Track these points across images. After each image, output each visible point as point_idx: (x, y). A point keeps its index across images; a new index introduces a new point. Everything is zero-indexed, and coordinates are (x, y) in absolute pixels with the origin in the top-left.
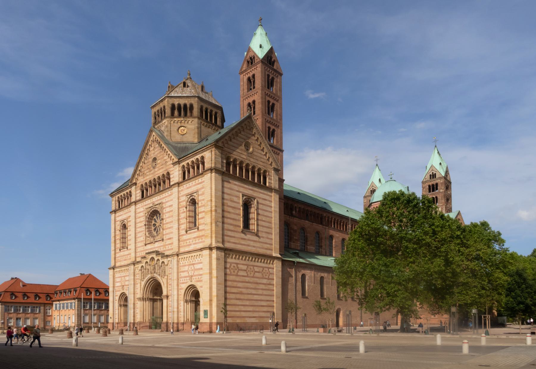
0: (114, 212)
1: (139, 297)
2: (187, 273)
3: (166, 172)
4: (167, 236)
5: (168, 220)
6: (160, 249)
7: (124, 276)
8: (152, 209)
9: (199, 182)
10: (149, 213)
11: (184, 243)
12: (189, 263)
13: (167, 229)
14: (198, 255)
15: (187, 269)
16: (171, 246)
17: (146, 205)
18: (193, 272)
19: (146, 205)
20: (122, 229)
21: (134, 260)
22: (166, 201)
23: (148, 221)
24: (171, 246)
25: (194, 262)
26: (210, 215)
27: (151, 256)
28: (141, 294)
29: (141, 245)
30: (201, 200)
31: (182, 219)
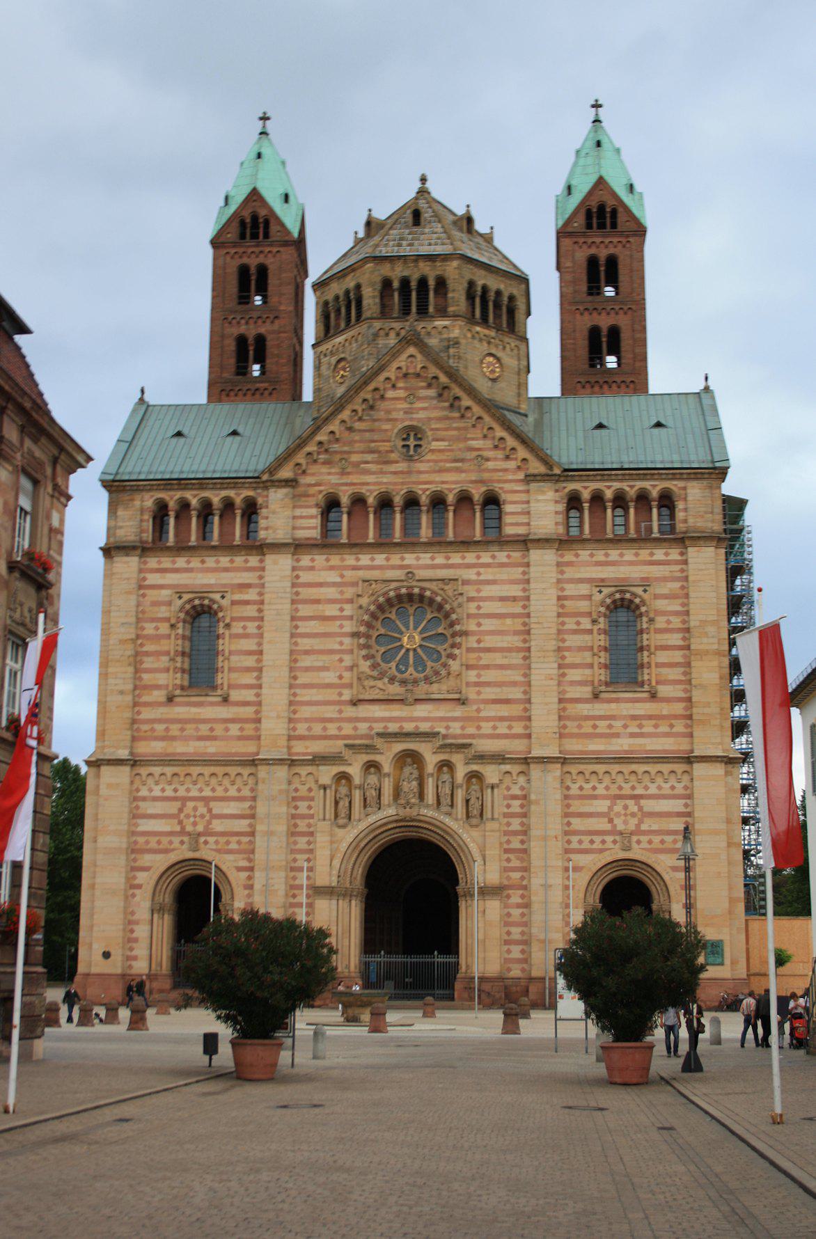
0: (139, 552)
1: (327, 884)
2: (606, 820)
3: (484, 489)
4: (488, 690)
5: (489, 641)
7: (206, 800)
9: (655, 558)
10: (381, 599)
11: (580, 727)
12: (614, 791)
13: (487, 667)
14: (666, 773)
15: (605, 809)
16: (510, 727)
17: (355, 568)
18: (633, 822)
19: (355, 568)
20: (184, 621)
21: (283, 742)
22: (482, 578)
23: (369, 626)
24: (510, 727)
25: (639, 791)
26: (715, 663)
27: (399, 747)
28: (335, 872)
29: (320, 698)
30: (664, 613)
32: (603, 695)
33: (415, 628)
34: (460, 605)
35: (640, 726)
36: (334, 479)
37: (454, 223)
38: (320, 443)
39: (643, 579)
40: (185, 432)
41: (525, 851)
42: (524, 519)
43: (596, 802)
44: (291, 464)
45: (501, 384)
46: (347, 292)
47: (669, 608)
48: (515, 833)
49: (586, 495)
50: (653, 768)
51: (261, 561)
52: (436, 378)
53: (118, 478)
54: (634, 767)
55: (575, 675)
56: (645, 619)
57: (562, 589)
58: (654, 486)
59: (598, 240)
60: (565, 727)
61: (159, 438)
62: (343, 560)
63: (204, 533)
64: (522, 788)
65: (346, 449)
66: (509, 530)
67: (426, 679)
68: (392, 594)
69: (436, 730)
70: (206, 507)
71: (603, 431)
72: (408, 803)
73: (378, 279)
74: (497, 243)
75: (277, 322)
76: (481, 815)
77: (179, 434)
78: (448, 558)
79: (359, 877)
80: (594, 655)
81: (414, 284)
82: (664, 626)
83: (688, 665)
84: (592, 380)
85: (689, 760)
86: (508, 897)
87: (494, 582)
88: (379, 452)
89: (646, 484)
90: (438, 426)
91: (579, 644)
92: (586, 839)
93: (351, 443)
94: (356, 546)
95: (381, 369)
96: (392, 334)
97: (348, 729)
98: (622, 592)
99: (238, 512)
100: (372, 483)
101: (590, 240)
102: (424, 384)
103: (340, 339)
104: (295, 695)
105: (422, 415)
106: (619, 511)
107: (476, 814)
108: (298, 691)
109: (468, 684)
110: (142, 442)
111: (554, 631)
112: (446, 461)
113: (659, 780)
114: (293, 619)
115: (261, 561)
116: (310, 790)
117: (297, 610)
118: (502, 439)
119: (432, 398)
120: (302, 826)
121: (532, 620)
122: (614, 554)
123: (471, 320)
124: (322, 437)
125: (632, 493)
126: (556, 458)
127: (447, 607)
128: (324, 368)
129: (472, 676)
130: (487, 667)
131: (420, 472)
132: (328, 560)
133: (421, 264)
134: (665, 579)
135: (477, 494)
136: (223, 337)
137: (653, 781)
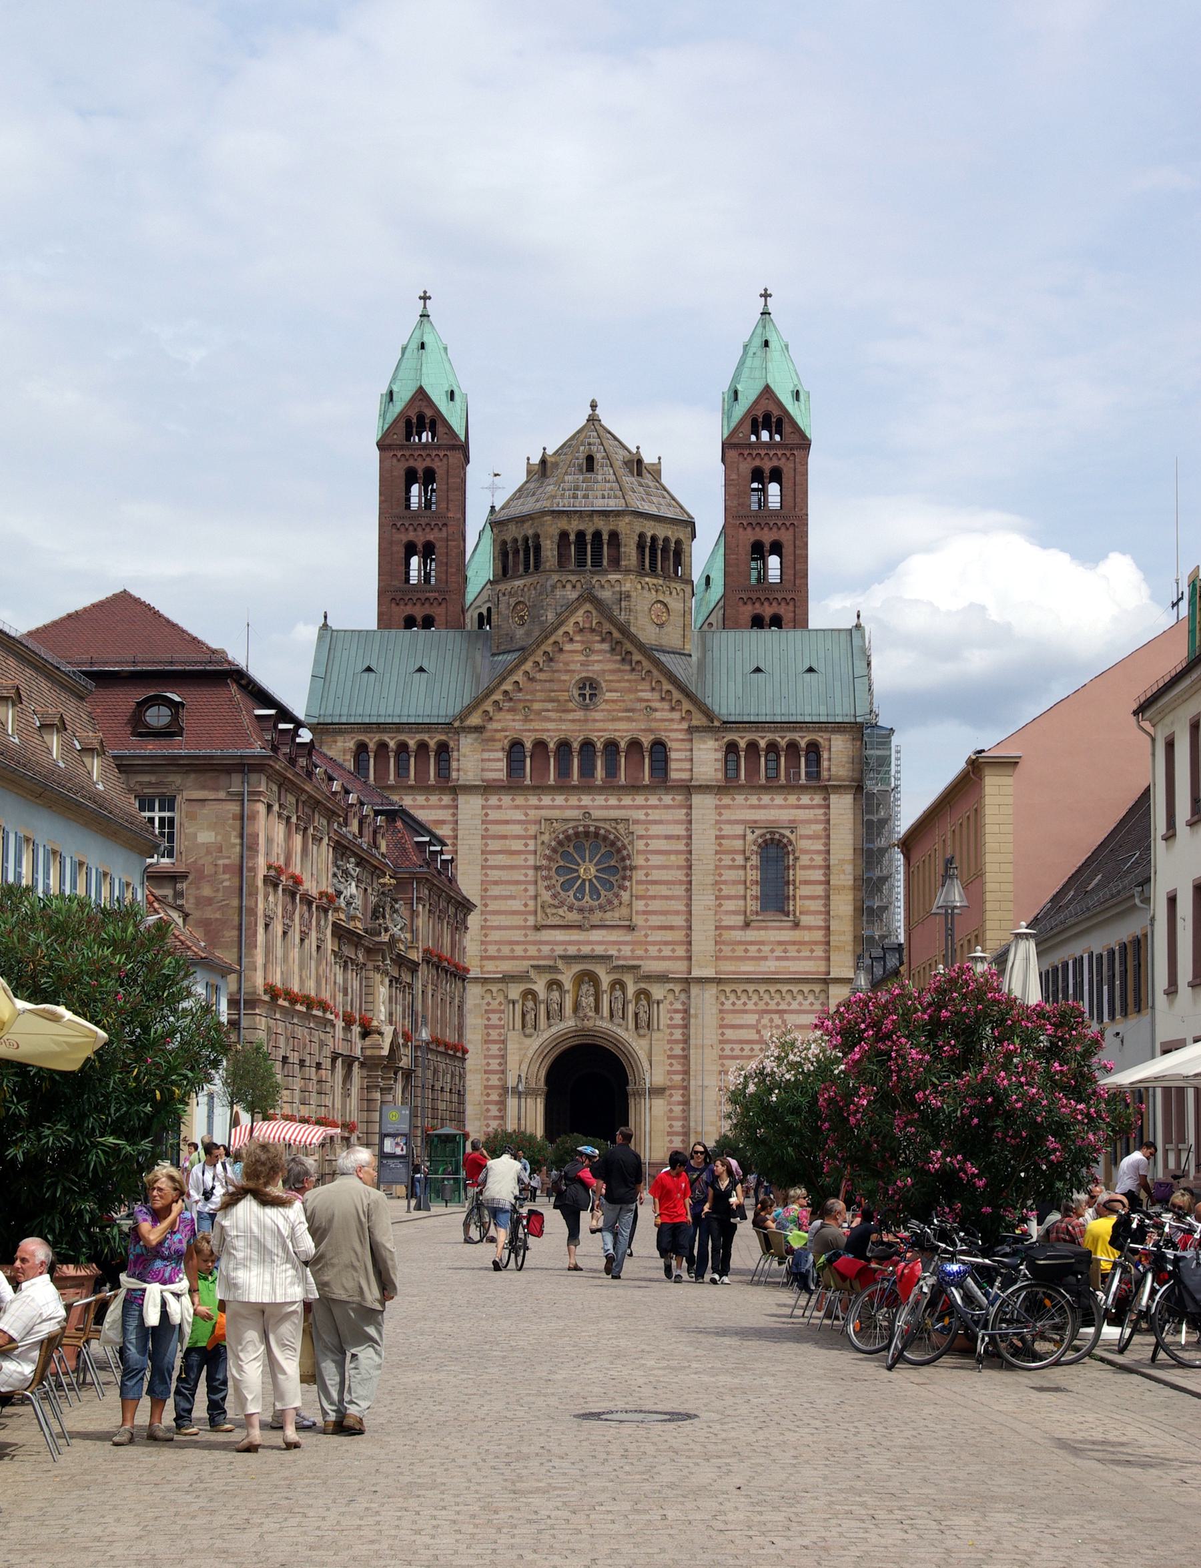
4: (654, 917)
5: (656, 875)
6: (619, 951)
8: (577, 827)
9: (801, 802)
10: (561, 836)
11: (733, 950)
12: (761, 1006)
13: (654, 897)
16: (673, 951)
17: (537, 808)
19: (537, 808)
23: (550, 859)
24: (673, 951)
25: (783, 1007)
27: (576, 968)
29: (507, 923)
30: (806, 852)
31: (725, 883)
32: (752, 924)
33: (591, 861)
34: (631, 842)
35: (785, 951)
36: (518, 725)
37: (625, 463)
38: (506, 692)
39: (791, 821)
40: (374, 667)
41: (686, 1058)
42: (687, 765)
43: (745, 1016)
44: (480, 711)
45: (666, 629)
46: (526, 539)
47: (813, 848)
48: (676, 1042)
49: (742, 744)
50: (795, 989)
51: (454, 800)
52: (610, 633)
53: (321, 721)
54: (779, 986)
55: (730, 905)
56: (791, 857)
57: (720, 829)
58: (802, 737)
59: (763, 452)
60: (721, 950)
61: (350, 673)
62: (527, 800)
63: (402, 770)
64: (683, 1003)
65: (528, 697)
66: (674, 775)
67: (601, 907)
68: (571, 832)
69: (610, 953)
70: (403, 747)
71: (760, 675)
72: (585, 1016)
73: (556, 532)
74: (664, 481)
75: (444, 529)
76: (648, 1026)
77: (369, 669)
78: (620, 800)
79: (543, 1079)
80: (746, 888)
81: (589, 538)
82: (808, 863)
83: (828, 897)
84: (754, 597)
85: (826, 981)
86: (671, 1096)
87: (660, 822)
88: (559, 701)
89: (796, 736)
90: (611, 678)
91: (733, 878)
92: (737, 1047)
93: (534, 692)
94: (540, 789)
95: (561, 624)
96: (569, 586)
97: (532, 950)
98: (771, 833)
99: (432, 754)
100: (552, 729)
101: (754, 453)
102: (598, 638)
103: (518, 583)
104: (486, 920)
105: (597, 667)
106: (772, 756)
107: (644, 1025)
108: (488, 917)
109: (637, 913)
110: (334, 678)
111: (712, 867)
112: (619, 711)
113: (800, 998)
114: (483, 852)
115: (454, 800)
116: (500, 1004)
117: (486, 845)
118: (668, 691)
119: (606, 652)
120: (494, 1034)
121: (693, 857)
122: (766, 799)
123: (641, 572)
124: (507, 686)
125: (783, 743)
126: (716, 709)
127: (619, 844)
128: (502, 606)
129: (639, 905)
130: (654, 897)
131: (596, 721)
132: (513, 800)
133: (596, 519)
134: (809, 822)
135: (646, 741)
136: (391, 543)
137: (794, 998)
